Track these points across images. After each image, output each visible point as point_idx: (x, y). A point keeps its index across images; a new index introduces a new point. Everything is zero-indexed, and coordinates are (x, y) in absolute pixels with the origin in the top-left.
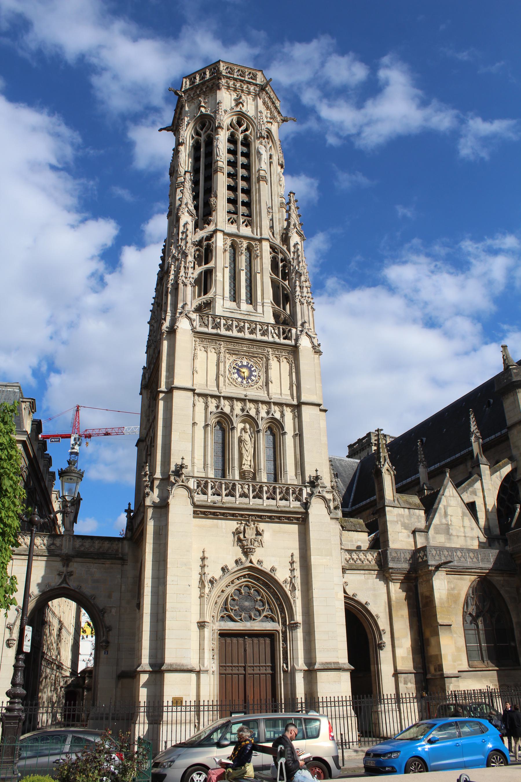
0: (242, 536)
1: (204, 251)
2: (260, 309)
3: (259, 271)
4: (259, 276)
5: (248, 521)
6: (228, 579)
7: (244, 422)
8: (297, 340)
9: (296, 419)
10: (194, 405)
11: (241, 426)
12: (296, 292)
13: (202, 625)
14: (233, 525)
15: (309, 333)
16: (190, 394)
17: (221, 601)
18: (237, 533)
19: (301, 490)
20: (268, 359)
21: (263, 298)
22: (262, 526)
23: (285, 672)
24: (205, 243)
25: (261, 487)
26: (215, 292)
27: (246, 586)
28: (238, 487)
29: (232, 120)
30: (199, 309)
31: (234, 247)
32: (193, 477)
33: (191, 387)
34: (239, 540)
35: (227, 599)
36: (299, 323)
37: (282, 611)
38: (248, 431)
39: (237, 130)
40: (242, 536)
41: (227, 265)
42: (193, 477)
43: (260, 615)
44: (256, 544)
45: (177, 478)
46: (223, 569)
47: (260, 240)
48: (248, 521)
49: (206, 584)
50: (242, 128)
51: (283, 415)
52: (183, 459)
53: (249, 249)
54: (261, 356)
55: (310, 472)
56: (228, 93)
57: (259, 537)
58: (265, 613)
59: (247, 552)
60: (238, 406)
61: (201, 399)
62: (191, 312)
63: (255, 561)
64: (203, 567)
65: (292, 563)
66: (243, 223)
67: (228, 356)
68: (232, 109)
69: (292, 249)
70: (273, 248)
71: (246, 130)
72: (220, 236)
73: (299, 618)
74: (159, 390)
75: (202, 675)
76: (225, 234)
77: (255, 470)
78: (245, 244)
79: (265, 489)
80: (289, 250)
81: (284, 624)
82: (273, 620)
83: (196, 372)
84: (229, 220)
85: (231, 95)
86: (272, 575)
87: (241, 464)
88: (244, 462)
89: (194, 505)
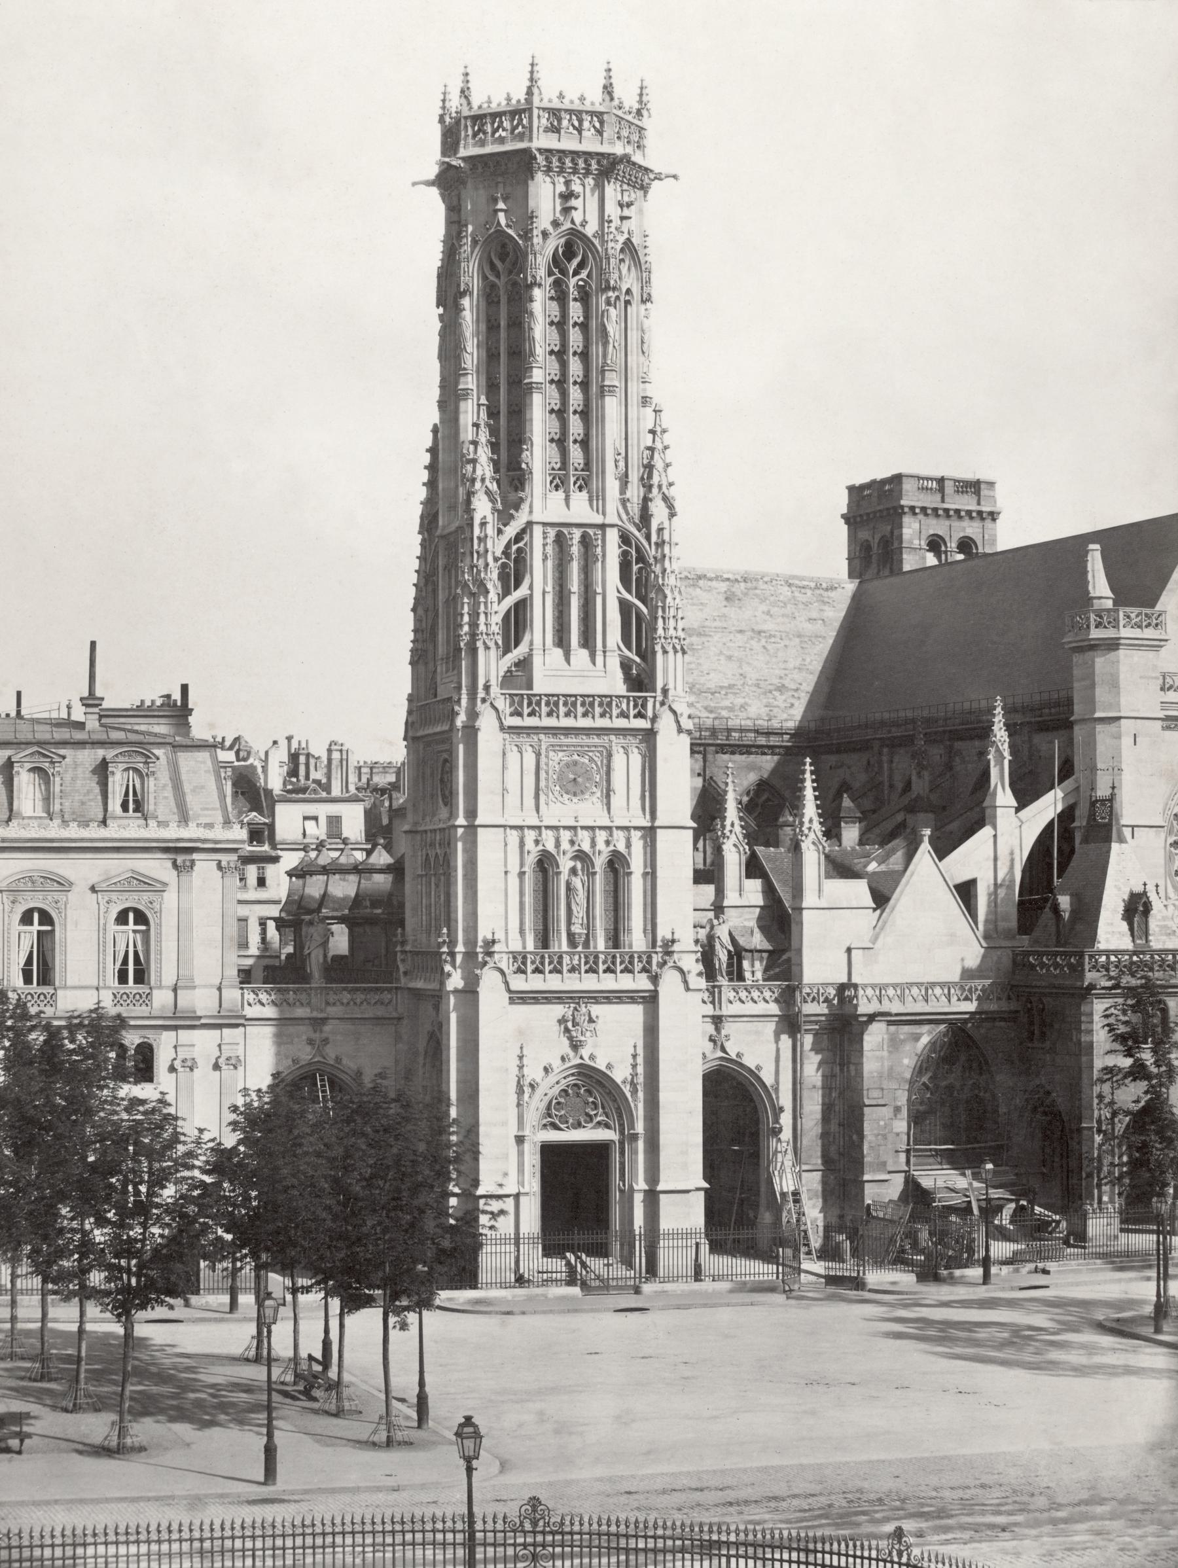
0: (570, 1025)
2: (599, 659)
4: (599, 599)
5: (578, 1003)
6: (552, 1078)
7: (574, 858)
8: (654, 720)
9: (648, 849)
11: (572, 864)
12: (655, 630)
13: (520, 1140)
14: (559, 1010)
15: (674, 707)
17: (543, 1105)
18: (562, 1021)
19: (650, 957)
20: (610, 755)
21: (604, 646)
22: (596, 1010)
23: (622, 1191)
24: (514, 548)
25: (596, 957)
26: (531, 643)
27: (575, 1085)
28: (566, 960)
29: (557, 249)
30: (508, 679)
34: (567, 1030)
35: (550, 1102)
36: (659, 685)
37: (620, 1116)
38: (580, 872)
39: (564, 272)
40: (570, 1025)
43: (591, 1120)
44: (588, 1034)
45: (488, 959)
46: (546, 1070)
47: (603, 527)
48: (578, 1003)
49: (525, 1089)
50: (575, 262)
51: (628, 845)
55: (663, 932)
56: (548, 179)
57: (593, 1025)
58: (599, 1119)
59: (575, 1046)
60: (566, 836)
61: (514, 832)
63: (586, 1057)
64: (521, 1067)
65: (634, 1056)
66: (575, 483)
68: (556, 224)
69: (654, 538)
70: (625, 539)
71: (581, 265)
72: (538, 531)
73: (640, 1127)
75: (522, 1199)
77: (588, 929)
78: (577, 534)
79: (602, 957)
81: (622, 1132)
82: (607, 1126)
85: (554, 184)
86: (608, 1072)
87: (569, 923)
88: (574, 920)
89: (509, 991)
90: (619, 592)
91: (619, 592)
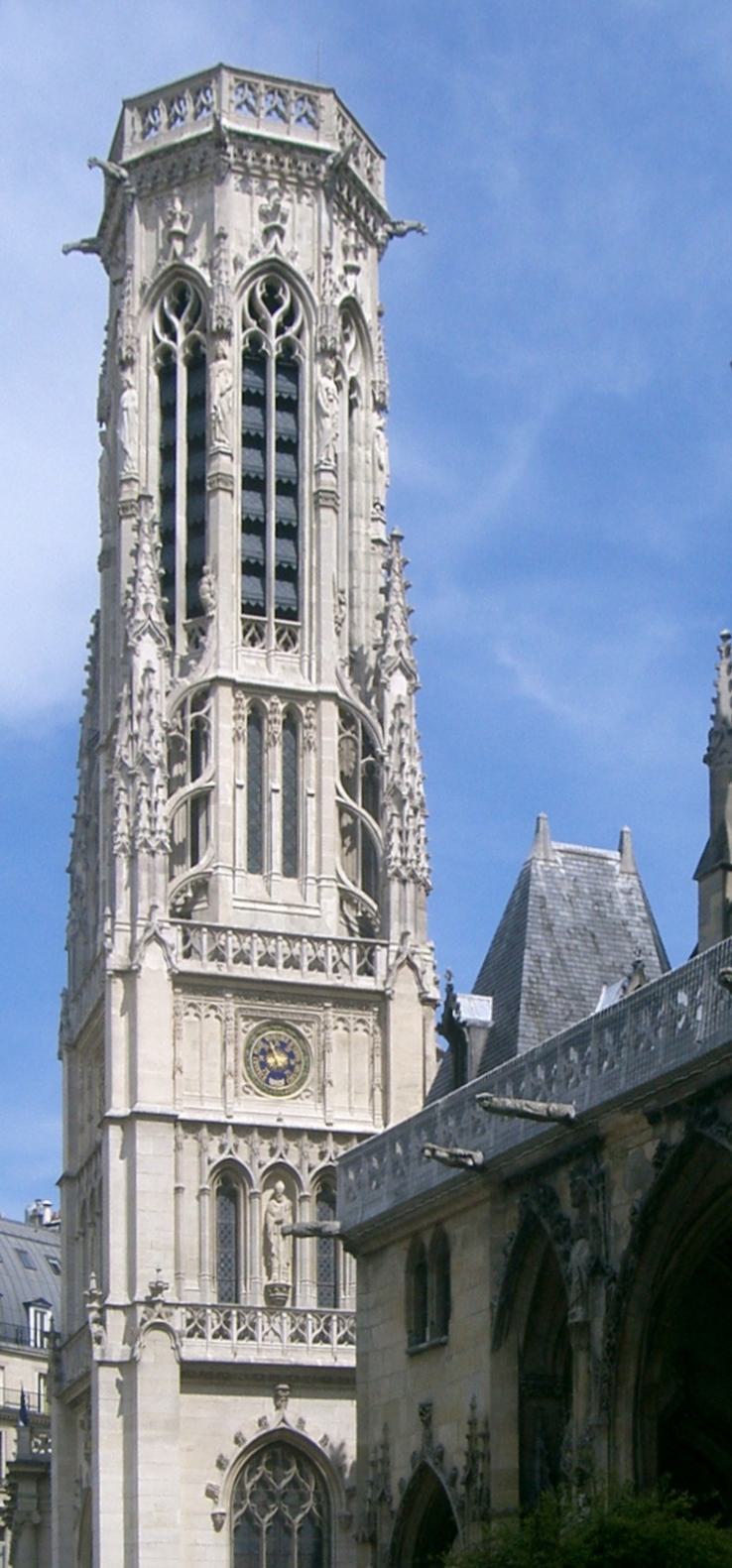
1: (189, 741)
2: (312, 890)
3: (312, 791)
10: (178, 1147)
16: (168, 1126)
24: (190, 717)
31: (256, 719)
32: (177, 1306)
33: (169, 1110)
41: (242, 781)
42: (177, 1306)
47: (318, 696)
52: (159, 1270)
53: (291, 723)
54: (309, 1019)
62: (167, 925)
67: (243, 1024)
69: (389, 718)
70: (347, 717)
74: (108, 1114)
76: (235, 685)
80: (381, 721)
83: (180, 1069)
84: (245, 633)
90: (338, 794)
91: (338, 794)
